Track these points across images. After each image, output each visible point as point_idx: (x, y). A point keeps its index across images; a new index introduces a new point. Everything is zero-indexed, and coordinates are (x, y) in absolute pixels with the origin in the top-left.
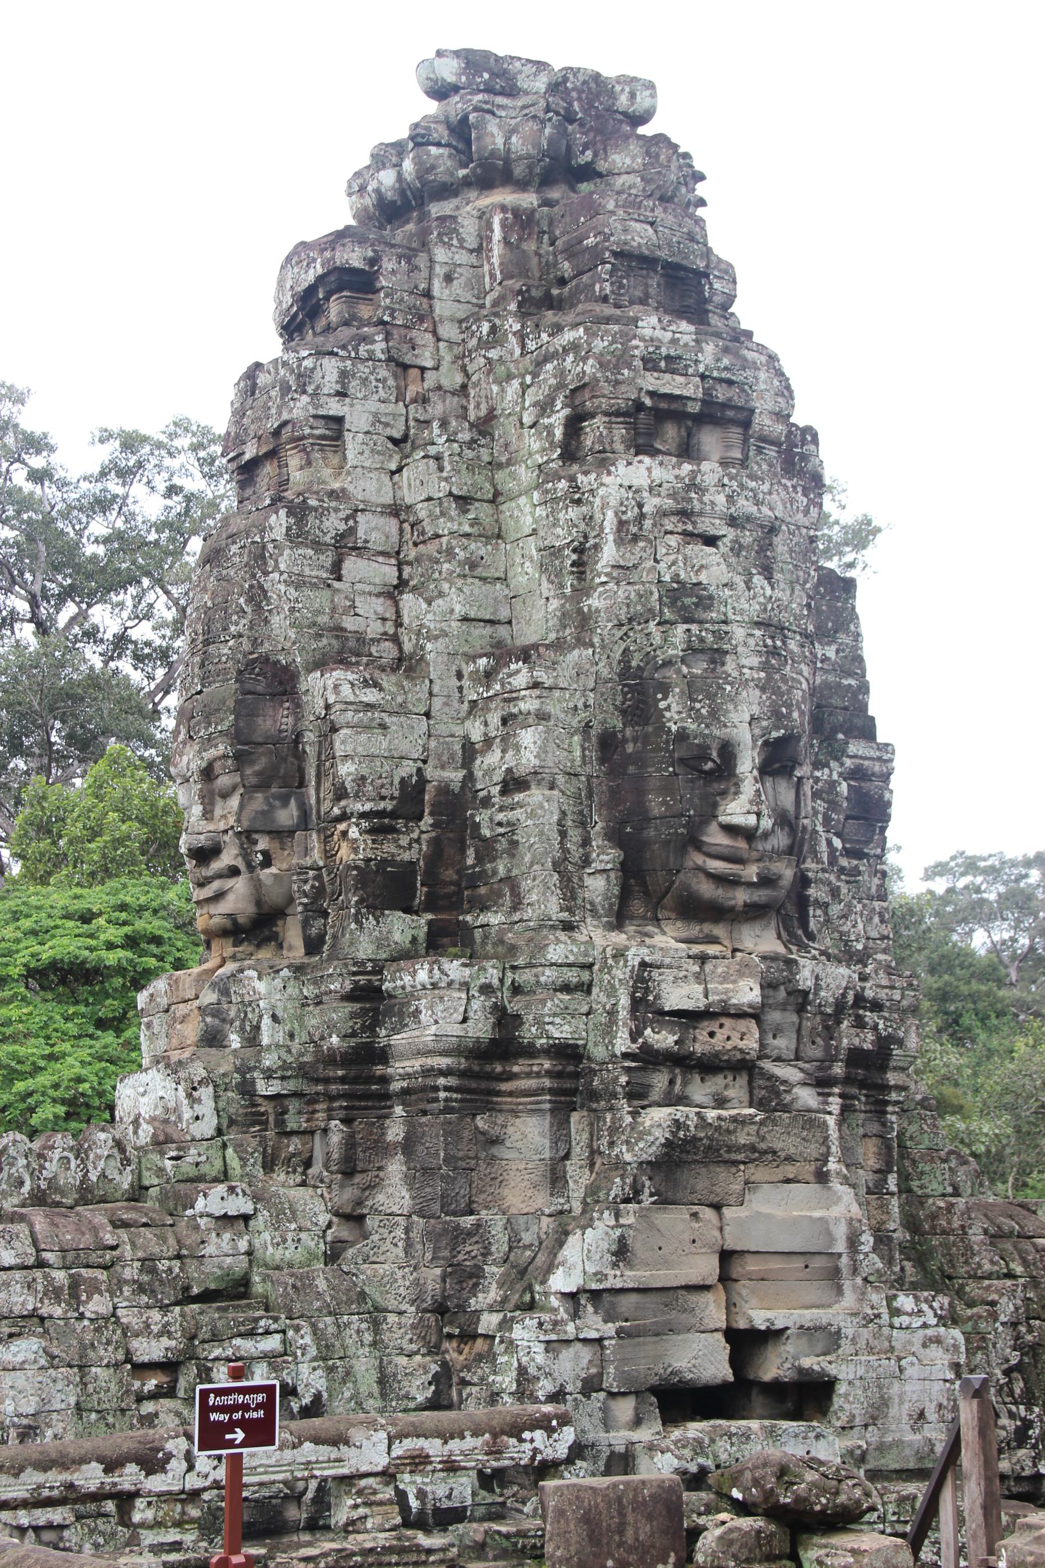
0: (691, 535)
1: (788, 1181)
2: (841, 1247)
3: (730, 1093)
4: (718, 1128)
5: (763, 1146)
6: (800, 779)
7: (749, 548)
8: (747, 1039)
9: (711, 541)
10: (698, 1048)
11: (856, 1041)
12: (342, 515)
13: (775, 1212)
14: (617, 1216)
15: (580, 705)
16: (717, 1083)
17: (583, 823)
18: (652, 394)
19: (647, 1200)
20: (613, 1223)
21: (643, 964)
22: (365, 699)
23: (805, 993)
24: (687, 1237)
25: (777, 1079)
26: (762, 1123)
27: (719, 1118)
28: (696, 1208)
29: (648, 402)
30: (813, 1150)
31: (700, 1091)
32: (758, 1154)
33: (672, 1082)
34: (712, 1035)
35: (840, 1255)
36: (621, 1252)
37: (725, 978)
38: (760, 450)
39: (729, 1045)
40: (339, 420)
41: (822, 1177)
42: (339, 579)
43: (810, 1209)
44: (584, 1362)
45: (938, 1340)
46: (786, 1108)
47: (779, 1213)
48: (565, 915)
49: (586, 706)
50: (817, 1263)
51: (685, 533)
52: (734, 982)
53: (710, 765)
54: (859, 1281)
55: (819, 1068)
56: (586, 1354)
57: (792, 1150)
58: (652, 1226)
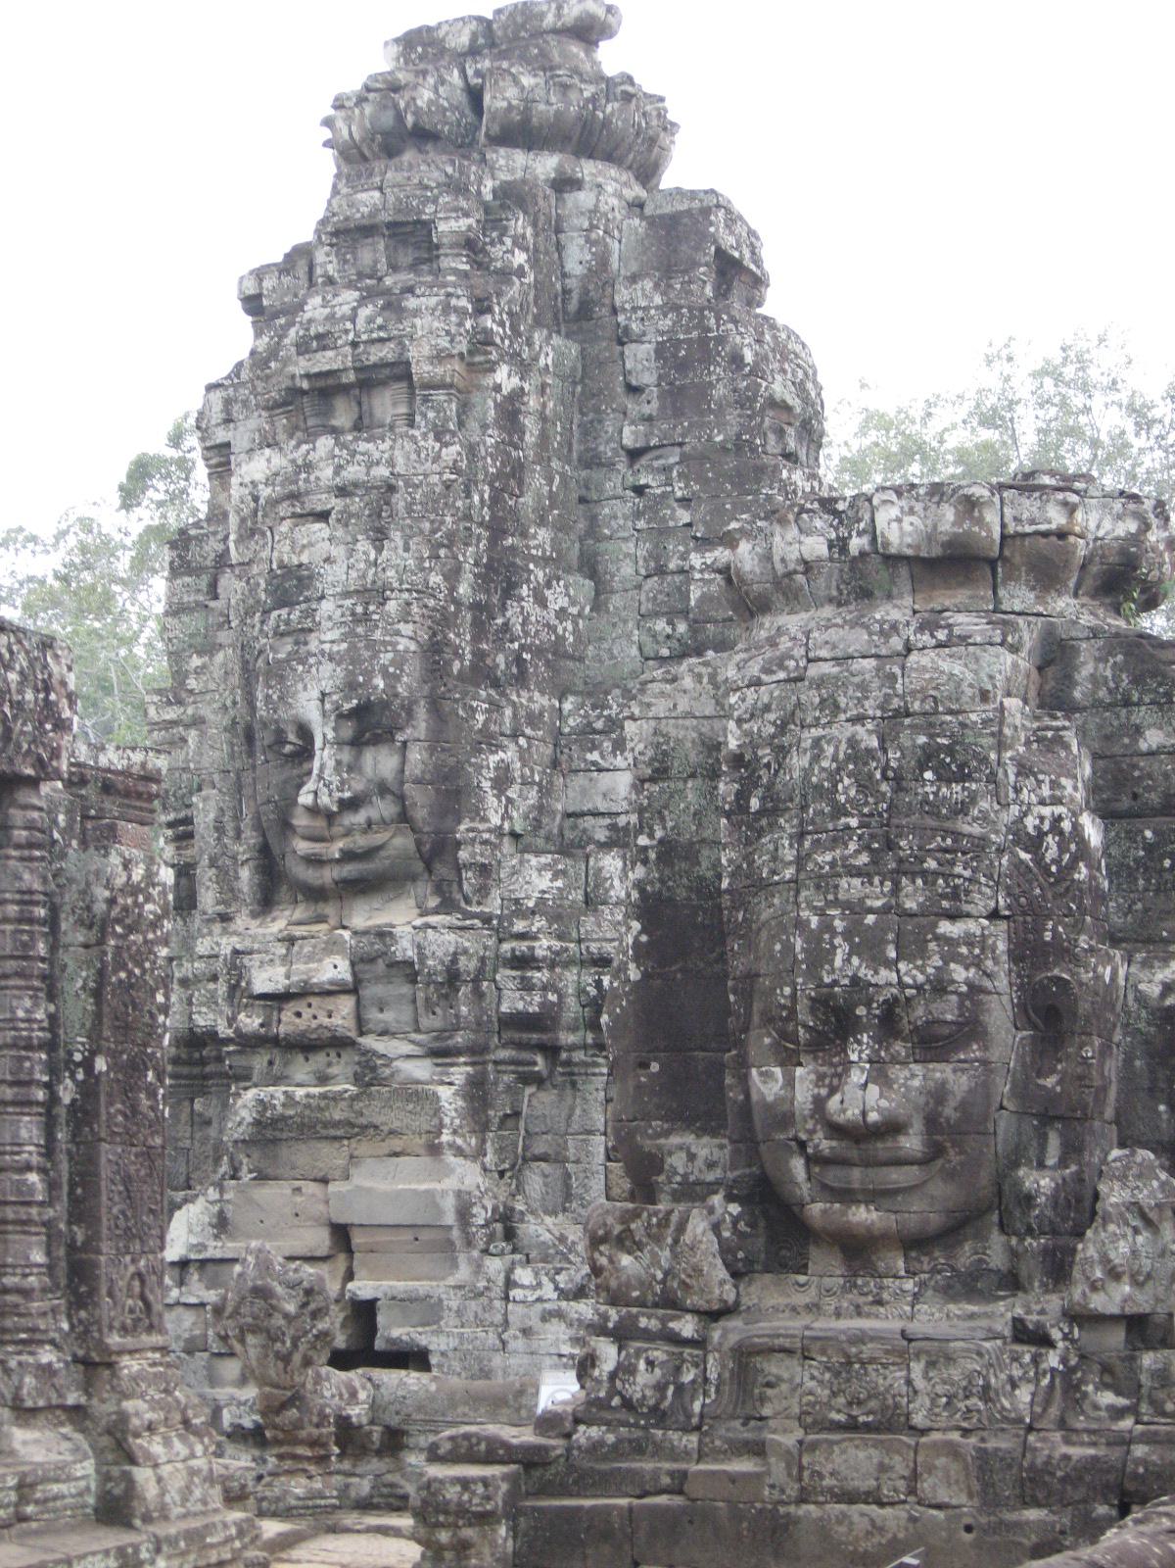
0: (301, 516)
1: (396, 1154)
2: (450, 1219)
3: (334, 1070)
4: (308, 1106)
5: (363, 1121)
6: (405, 743)
7: (357, 516)
8: (341, 1015)
9: (323, 516)
10: (282, 1030)
11: (520, 1006)
12: (220, 537)
13: (383, 1186)
14: (222, 1192)
15: (229, 703)
16: (319, 1059)
17: (237, 818)
18: (308, 376)
19: (246, 1176)
20: (217, 1196)
21: (236, 952)
22: (168, 717)
23: (410, 964)
24: (288, 1211)
25: (375, 1053)
26: (354, 1098)
27: (308, 1096)
28: (297, 1183)
29: (305, 385)
30: (423, 1123)
31: (302, 1069)
32: (356, 1130)
33: (271, 1063)
34: (299, 1015)
35: (450, 1228)
36: (222, 1224)
37: (310, 958)
38: (426, 399)
39: (314, 1024)
40: (228, 445)
41: (434, 1150)
42: (216, 597)
43: (419, 1182)
44: (187, 1324)
45: (559, 1314)
46: (382, 1082)
47: (382, 1186)
48: (221, 908)
49: (235, 703)
50: (425, 1235)
51: (294, 515)
52: (320, 961)
53: (288, 748)
54: (476, 1253)
55: (436, 1039)
56: (189, 1318)
57: (396, 1125)
58: (250, 1201)
